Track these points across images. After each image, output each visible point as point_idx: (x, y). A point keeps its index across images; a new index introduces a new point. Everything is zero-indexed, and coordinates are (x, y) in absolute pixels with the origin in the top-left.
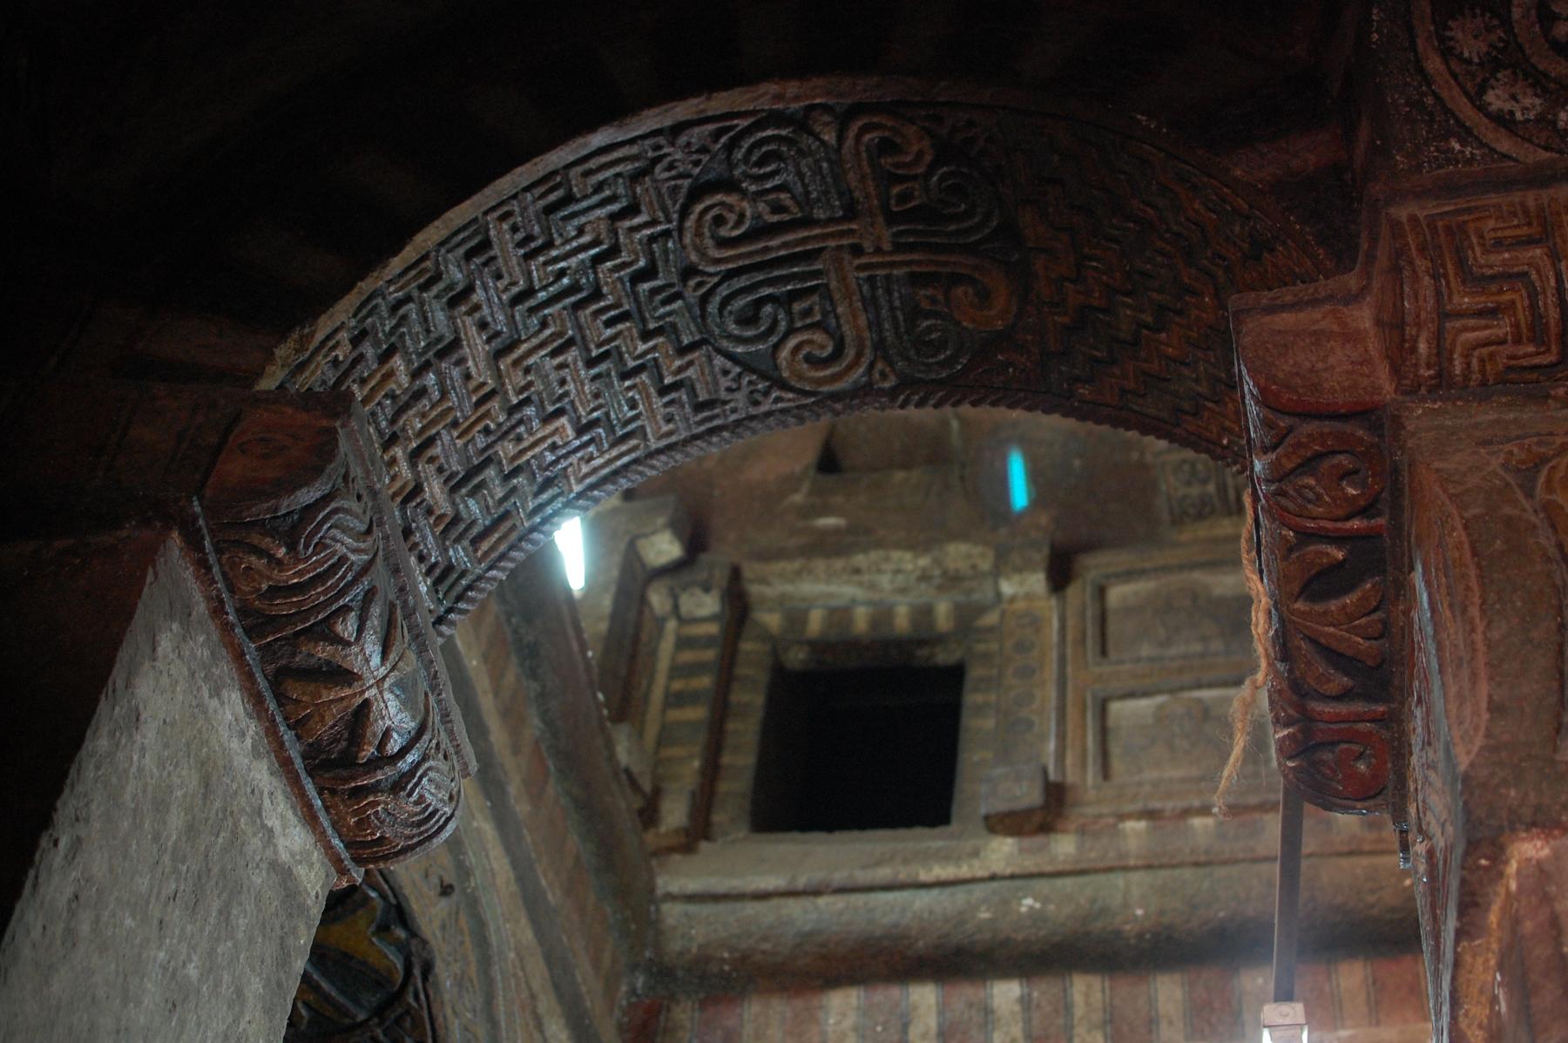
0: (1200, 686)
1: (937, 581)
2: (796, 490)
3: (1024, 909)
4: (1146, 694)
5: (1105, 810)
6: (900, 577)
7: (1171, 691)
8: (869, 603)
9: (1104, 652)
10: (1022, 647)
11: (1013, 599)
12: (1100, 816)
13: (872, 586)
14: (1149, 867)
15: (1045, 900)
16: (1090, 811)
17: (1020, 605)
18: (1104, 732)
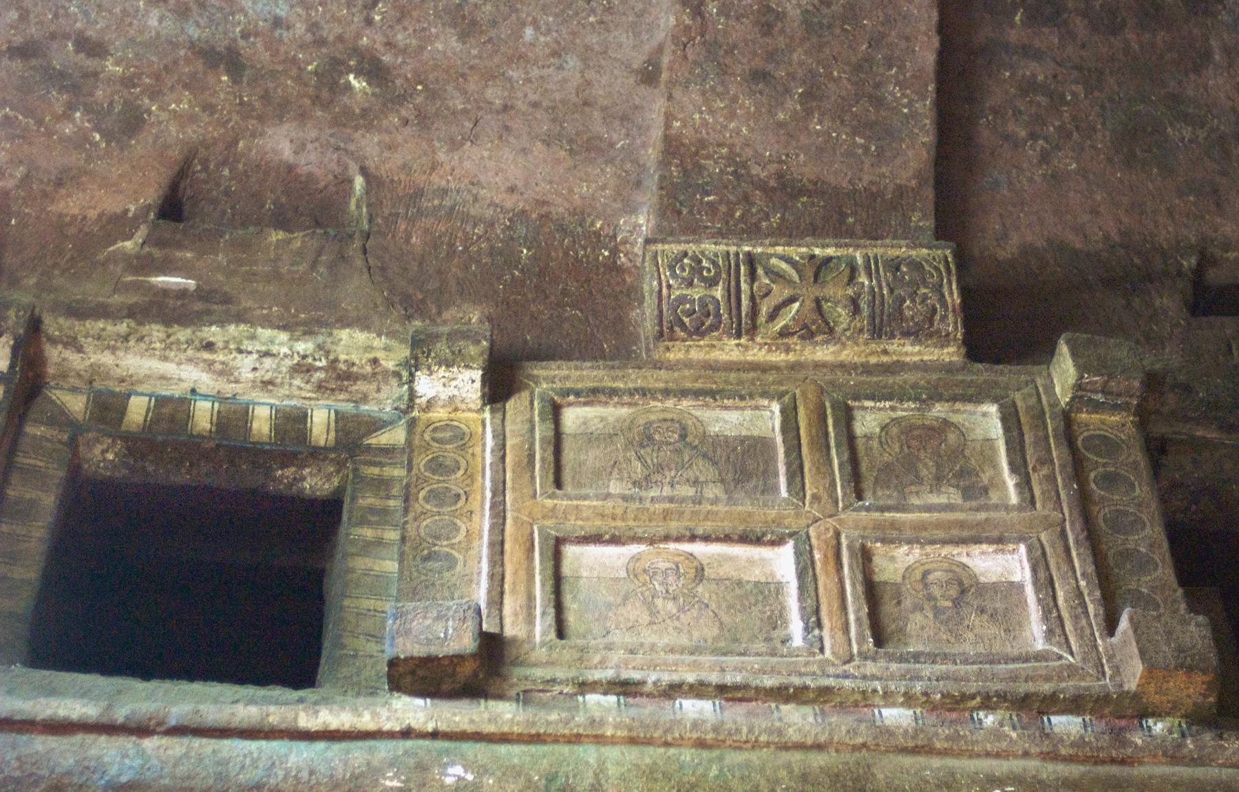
0: (693, 538)
1: (320, 375)
2: (129, 237)
3: (449, 781)
4: (615, 540)
5: (560, 674)
6: (268, 362)
7: (652, 541)
8: (219, 397)
9: (558, 483)
10: (437, 466)
11: (430, 404)
13: (226, 372)
14: (633, 741)
15: (482, 771)
16: (539, 673)
17: (439, 414)
18: (557, 582)
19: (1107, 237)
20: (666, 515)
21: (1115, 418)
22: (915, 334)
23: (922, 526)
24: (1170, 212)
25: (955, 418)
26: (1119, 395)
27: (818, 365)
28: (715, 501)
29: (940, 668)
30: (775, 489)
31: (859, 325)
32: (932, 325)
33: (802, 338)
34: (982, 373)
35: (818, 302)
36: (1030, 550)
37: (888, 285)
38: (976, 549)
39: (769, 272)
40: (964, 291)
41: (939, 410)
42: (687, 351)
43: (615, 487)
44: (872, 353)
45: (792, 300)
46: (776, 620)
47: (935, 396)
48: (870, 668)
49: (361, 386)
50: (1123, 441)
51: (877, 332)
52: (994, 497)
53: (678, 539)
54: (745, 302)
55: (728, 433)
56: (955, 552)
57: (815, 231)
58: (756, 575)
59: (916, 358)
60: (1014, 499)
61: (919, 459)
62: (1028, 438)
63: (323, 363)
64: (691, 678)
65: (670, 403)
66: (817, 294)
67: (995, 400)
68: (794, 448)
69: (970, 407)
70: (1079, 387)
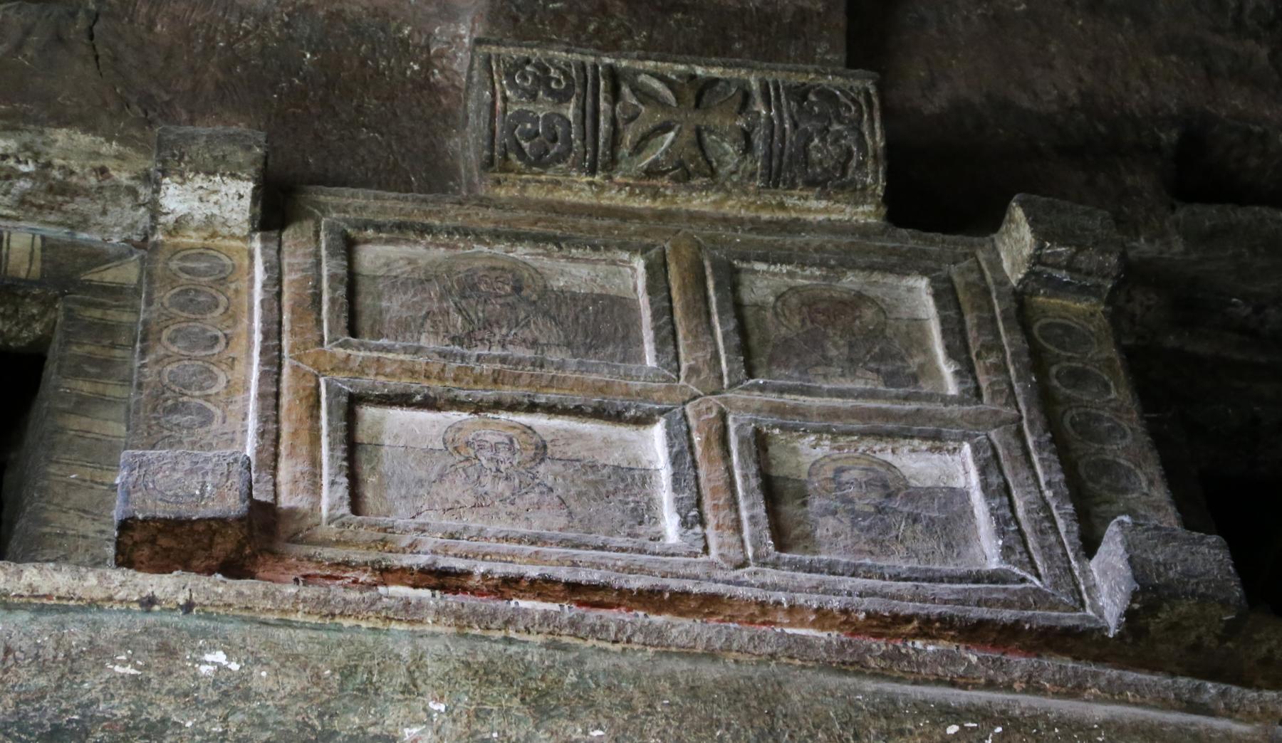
0: (532, 408)
1: (24, 184)
4: (429, 404)
5: (356, 556)
7: (478, 408)
9: (353, 331)
11: (180, 224)
12: (346, 564)
17: (192, 238)
19: (1063, 98)
20: (497, 379)
21: (1082, 306)
22: (820, 184)
23: (834, 414)
24: (1145, 75)
25: (872, 292)
26: (1089, 274)
27: (693, 217)
28: (561, 366)
29: (860, 583)
30: (640, 358)
31: (750, 167)
32: (844, 173)
33: (675, 179)
34: (908, 239)
35: (698, 132)
36: (976, 449)
37: (791, 116)
38: (905, 446)
39: (635, 90)
40: (888, 136)
41: (851, 281)
42: (524, 188)
43: (426, 341)
44: (765, 206)
45: (665, 128)
46: (643, 514)
47: (846, 263)
48: (771, 575)
49: (81, 205)
50: (1092, 334)
51: (775, 177)
52: (926, 387)
53: (513, 407)
54: (604, 125)
55: (576, 289)
56: (877, 448)
57: (691, 52)
58: (616, 458)
59: (821, 217)
60: (952, 389)
61: (826, 336)
62: (970, 320)
63: (30, 167)
64: (533, 572)
65: (499, 249)
66: (699, 122)
67: (924, 272)
68: (663, 312)
69: (891, 279)
70: (1037, 259)
